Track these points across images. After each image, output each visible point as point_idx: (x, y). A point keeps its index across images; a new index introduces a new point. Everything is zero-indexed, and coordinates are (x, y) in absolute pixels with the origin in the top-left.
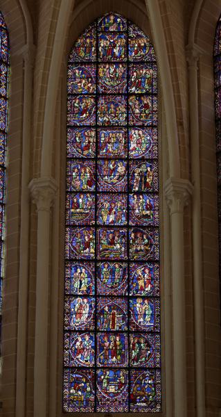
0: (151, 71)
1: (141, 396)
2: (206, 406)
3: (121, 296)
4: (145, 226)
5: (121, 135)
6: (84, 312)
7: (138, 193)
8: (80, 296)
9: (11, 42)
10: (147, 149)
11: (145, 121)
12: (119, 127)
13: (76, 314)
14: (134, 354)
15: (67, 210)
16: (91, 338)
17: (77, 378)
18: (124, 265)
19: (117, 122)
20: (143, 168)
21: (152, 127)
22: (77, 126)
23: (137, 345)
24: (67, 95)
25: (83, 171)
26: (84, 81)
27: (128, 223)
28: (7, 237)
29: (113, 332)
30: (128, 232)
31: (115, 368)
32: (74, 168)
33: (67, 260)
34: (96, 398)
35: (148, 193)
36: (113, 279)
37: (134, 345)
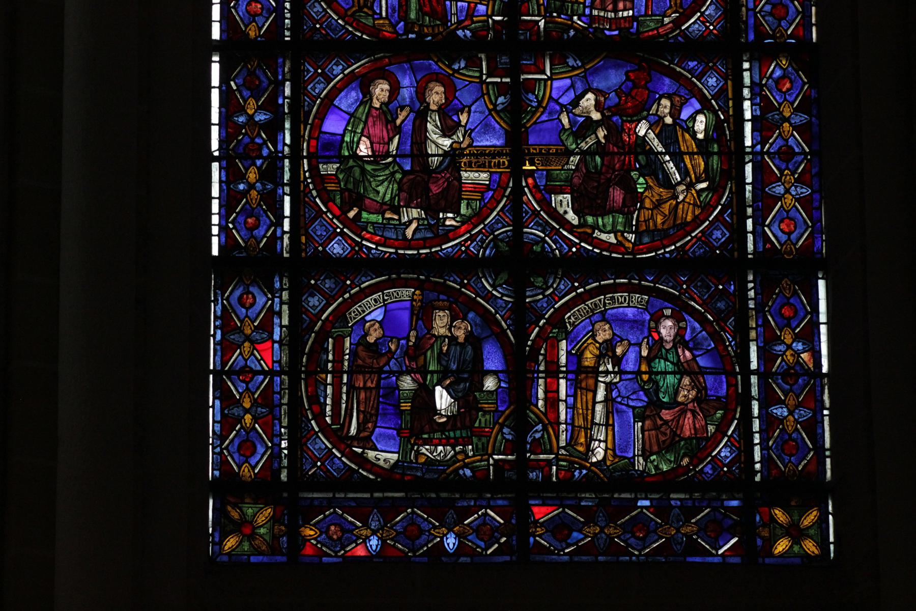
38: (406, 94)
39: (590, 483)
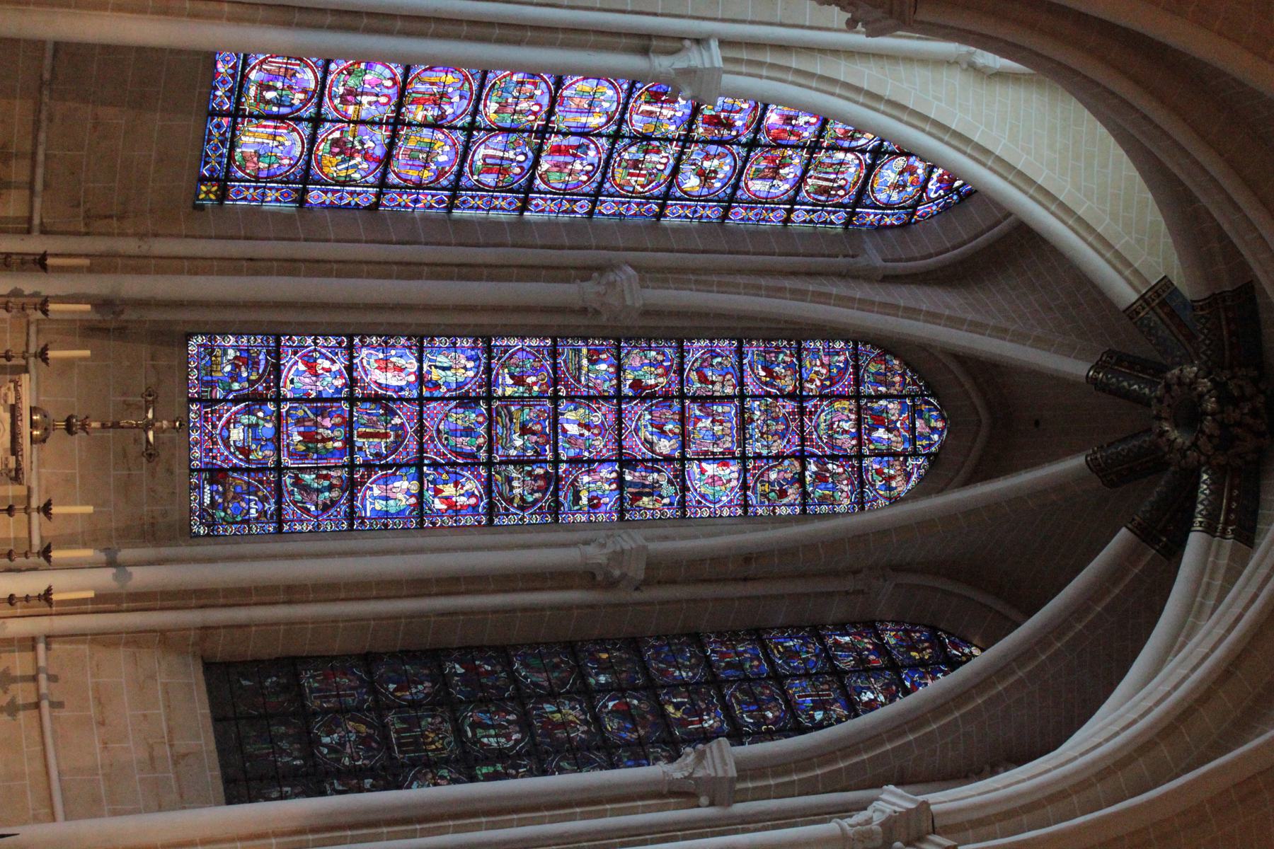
0: (847, 502)
1: (224, 495)
2: (206, 629)
3: (421, 450)
4: (557, 497)
5: (728, 445)
6: (389, 375)
7: (620, 481)
8: (420, 368)
9: (888, 233)
10: (703, 496)
12: (742, 442)
13: (386, 360)
14: (308, 478)
15: (585, 339)
16: (338, 390)
17: (258, 363)
18: (483, 455)
19: (751, 436)
20: (667, 490)
21: (745, 505)
22: (741, 359)
23: (326, 483)
24: (797, 334)
25: (660, 371)
26: (824, 371)
28: (528, 223)
29: (352, 436)
30: (545, 461)
31: (279, 439)
32: (664, 354)
33: (490, 341)
34: (219, 401)
35: (622, 499)
36: (454, 432)
37: (326, 477)
38: (386, 91)
39: (234, 135)
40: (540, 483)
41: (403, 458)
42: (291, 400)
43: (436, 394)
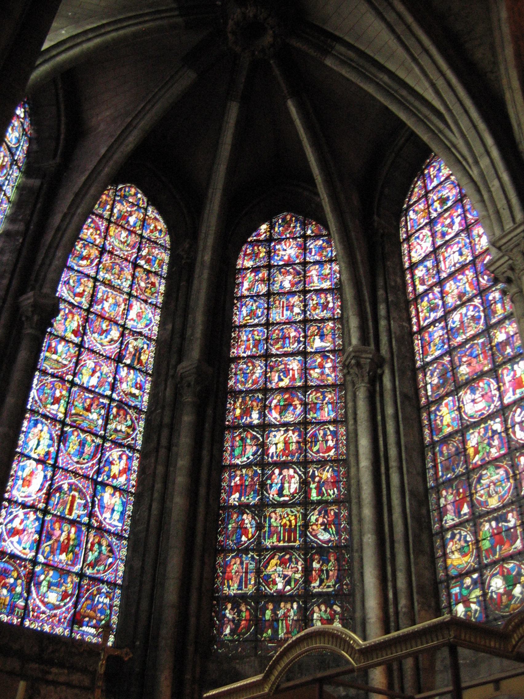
1: (91, 618)
3: (86, 477)
5: (121, 300)
7: (130, 367)
10: (147, 326)
11: (150, 298)
12: (120, 290)
13: (24, 480)
14: (91, 557)
19: (118, 285)
23: (96, 546)
27: (112, 394)
30: (109, 405)
35: (140, 370)
37: (93, 545)
40: (122, 413)
41: (91, 491)
42: (37, 552)
43: (53, 455)
